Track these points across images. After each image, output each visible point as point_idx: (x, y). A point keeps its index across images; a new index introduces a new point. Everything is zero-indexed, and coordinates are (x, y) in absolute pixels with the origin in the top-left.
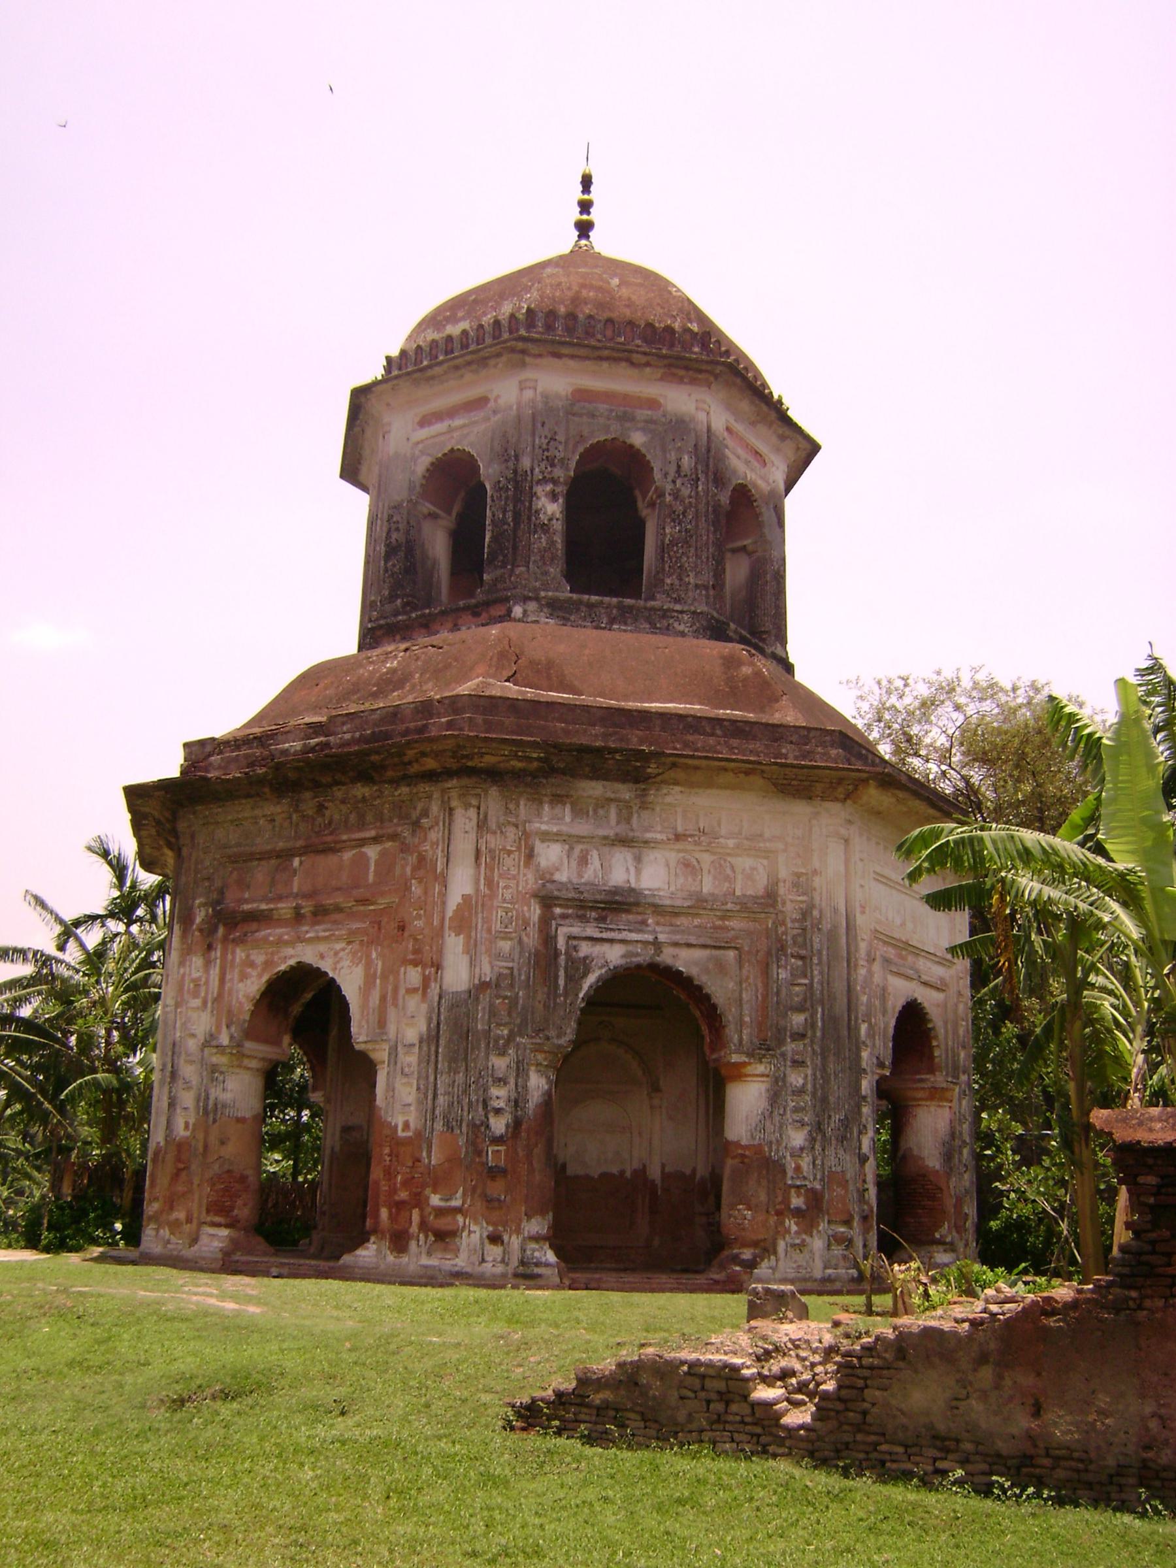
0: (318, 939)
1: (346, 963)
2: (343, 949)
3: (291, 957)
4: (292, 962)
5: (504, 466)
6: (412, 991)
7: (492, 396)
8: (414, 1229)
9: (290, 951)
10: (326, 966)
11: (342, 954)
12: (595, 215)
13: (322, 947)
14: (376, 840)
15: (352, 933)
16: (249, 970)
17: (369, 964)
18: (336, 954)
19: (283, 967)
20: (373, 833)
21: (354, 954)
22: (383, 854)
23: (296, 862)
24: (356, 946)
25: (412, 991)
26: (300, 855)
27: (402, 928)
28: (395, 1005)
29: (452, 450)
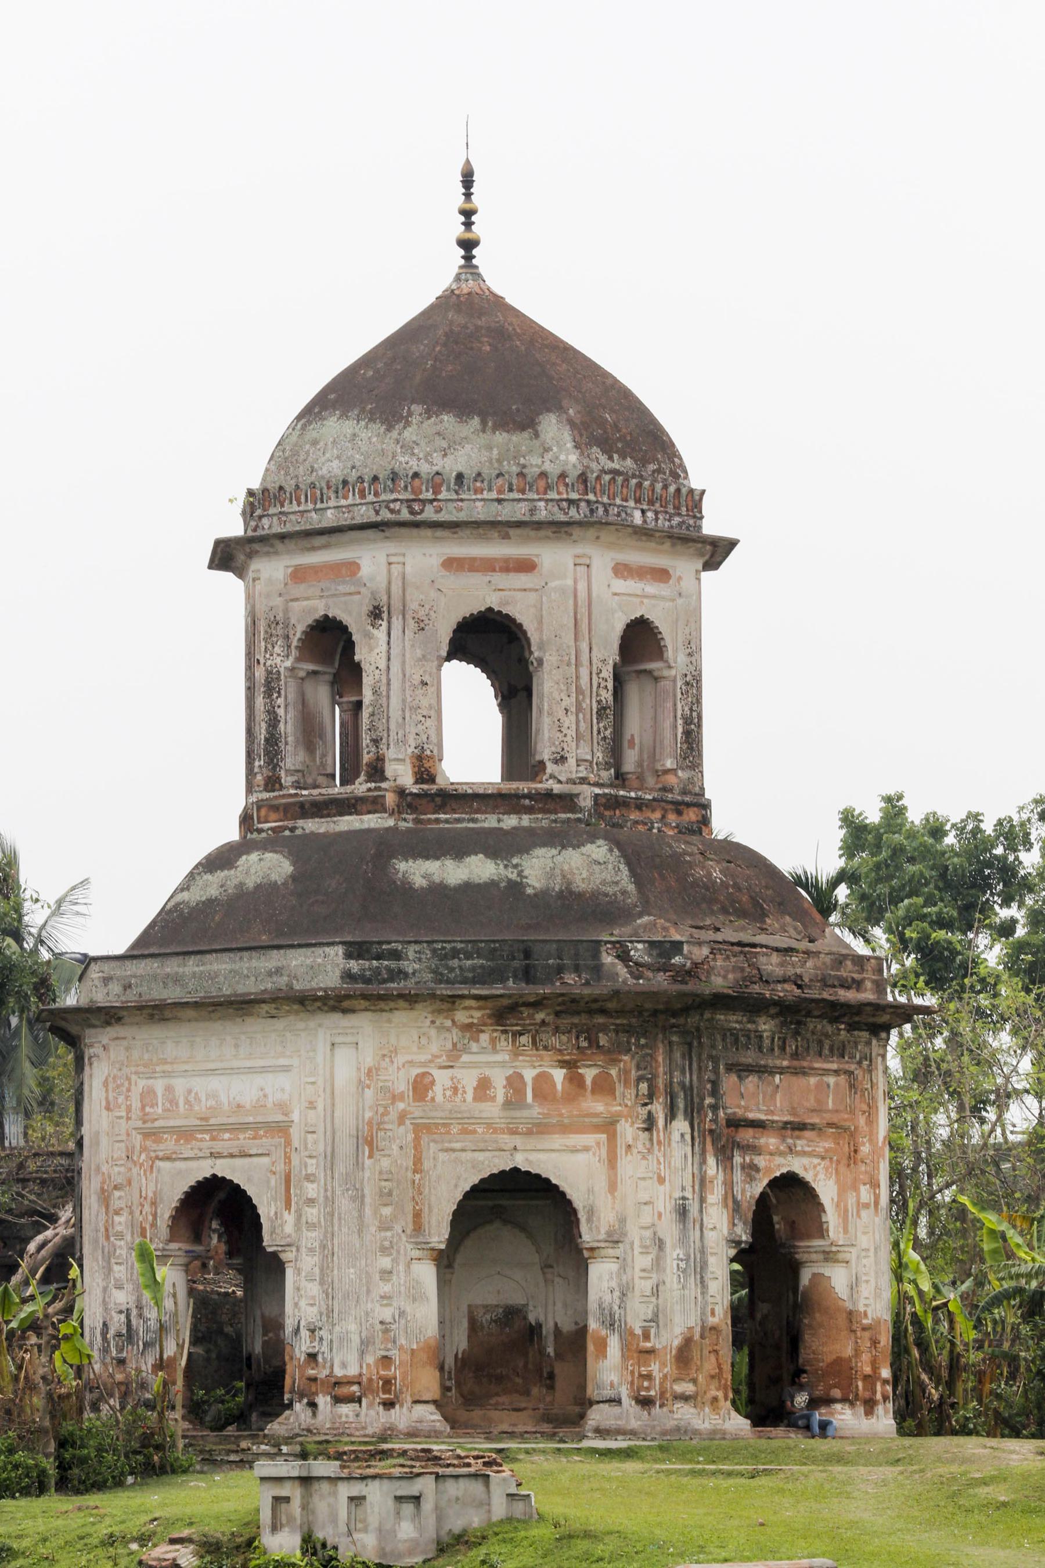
0: (804, 1154)
1: (821, 1176)
2: (819, 1164)
3: (783, 1166)
4: (784, 1170)
5: (689, 659)
6: (867, 1206)
7: (675, 573)
8: (879, 1396)
9: (779, 1160)
10: (808, 1177)
11: (818, 1168)
12: (479, 229)
13: (806, 1161)
14: (836, 1072)
15: (827, 1151)
16: (753, 1173)
17: (838, 1181)
18: (815, 1167)
19: (778, 1174)
20: (835, 1066)
21: (826, 1169)
22: (837, 1084)
23: (777, 1078)
24: (827, 1162)
25: (867, 1206)
26: (781, 1073)
27: (856, 1151)
28: (859, 1215)
29: (642, 616)
